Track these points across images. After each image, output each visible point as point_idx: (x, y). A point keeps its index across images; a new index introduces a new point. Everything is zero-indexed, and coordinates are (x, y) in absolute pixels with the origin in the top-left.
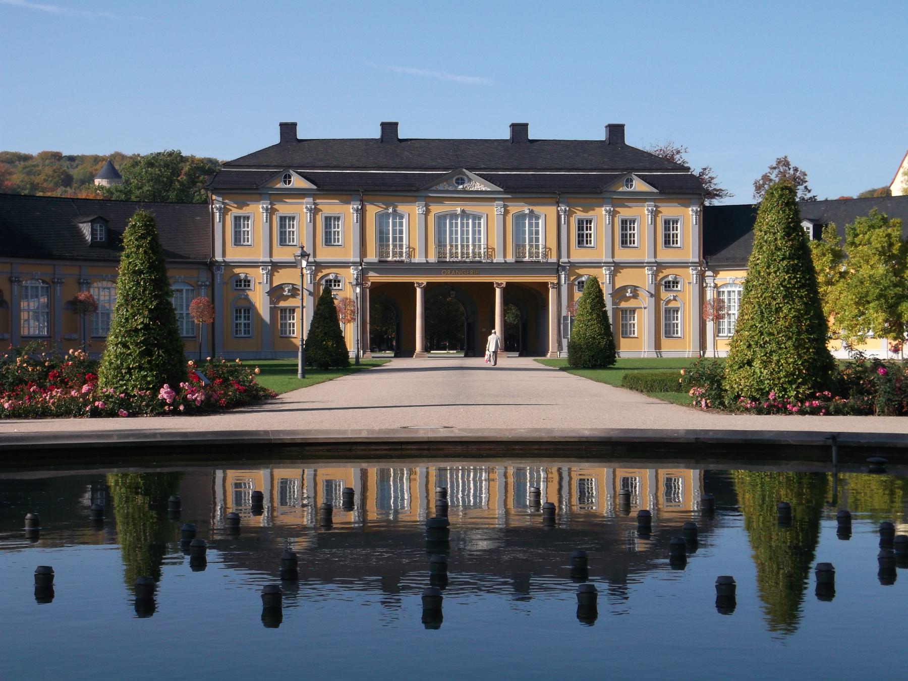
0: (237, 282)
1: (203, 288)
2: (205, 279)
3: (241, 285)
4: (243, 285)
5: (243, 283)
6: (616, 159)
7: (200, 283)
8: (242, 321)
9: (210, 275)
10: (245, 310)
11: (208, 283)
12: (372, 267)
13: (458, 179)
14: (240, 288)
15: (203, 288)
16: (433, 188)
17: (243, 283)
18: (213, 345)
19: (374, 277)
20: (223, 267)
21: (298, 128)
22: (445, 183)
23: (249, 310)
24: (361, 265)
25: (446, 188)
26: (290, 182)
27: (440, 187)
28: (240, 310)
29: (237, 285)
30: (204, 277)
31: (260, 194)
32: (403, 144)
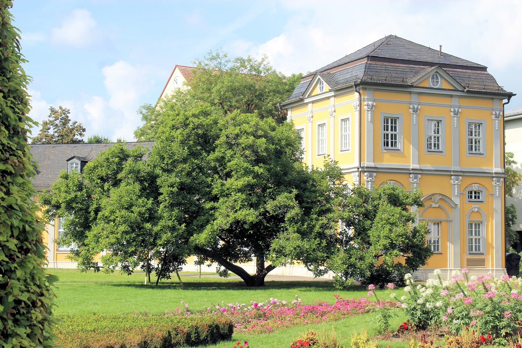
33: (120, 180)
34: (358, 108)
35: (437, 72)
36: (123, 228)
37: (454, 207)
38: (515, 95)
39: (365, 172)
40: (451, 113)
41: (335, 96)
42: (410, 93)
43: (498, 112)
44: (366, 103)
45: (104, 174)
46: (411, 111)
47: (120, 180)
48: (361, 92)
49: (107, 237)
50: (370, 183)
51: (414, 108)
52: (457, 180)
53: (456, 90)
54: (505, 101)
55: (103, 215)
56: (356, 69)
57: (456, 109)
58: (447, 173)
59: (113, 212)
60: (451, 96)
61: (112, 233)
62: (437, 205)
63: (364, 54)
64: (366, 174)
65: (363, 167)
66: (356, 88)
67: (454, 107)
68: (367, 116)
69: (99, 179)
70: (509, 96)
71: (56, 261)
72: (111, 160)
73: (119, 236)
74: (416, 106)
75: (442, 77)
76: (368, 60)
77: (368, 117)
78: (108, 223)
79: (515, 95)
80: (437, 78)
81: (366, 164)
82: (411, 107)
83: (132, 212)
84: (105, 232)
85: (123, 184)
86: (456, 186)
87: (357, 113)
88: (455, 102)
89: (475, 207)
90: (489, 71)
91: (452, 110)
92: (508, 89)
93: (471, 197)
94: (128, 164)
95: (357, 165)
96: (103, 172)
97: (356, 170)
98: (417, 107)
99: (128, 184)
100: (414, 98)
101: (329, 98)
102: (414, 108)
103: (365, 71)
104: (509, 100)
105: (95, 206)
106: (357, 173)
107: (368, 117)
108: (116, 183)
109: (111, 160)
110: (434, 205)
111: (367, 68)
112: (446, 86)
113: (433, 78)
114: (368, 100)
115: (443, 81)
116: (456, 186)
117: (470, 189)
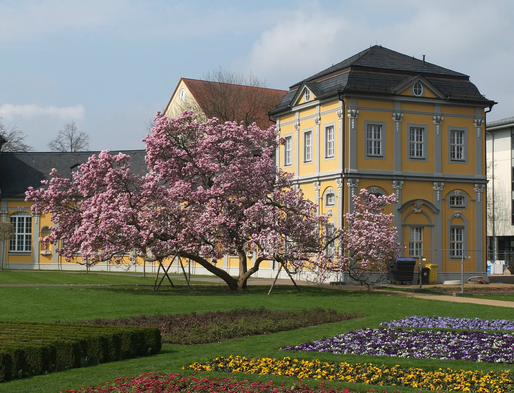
8: (25, 234)
34: (342, 116)
35: (419, 81)
37: (436, 212)
38: (497, 103)
39: (349, 178)
40: (434, 121)
41: (320, 105)
42: (393, 101)
43: (479, 120)
44: (349, 111)
46: (394, 118)
48: (345, 100)
50: (353, 189)
51: (397, 116)
52: (439, 186)
53: (438, 98)
54: (487, 109)
56: (340, 78)
57: (439, 117)
58: (430, 180)
60: (434, 104)
62: (420, 211)
63: (348, 64)
64: (349, 180)
65: (347, 174)
66: (339, 96)
67: (436, 116)
68: (351, 124)
70: (491, 104)
71: (61, 263)
74: (399, 114)
75: (424, 86)
76: (352, 69)
77: (351, 124)
79: (497, 103)
80: (420, 87)
81: (350, 170)
82: (394, 114)
86: (438, 192)
87: (341, 120)
88: (437, 110)
89: (457, 212)
90: (472, 80)
91: (435, 118)
92: (489, 97)
93: (453, 203)
95: (340, 171)
97: (340, 176)
98: (400, 115)
100: (398, 107)
101: (314, 106)
102: (397, 116)
103: (349, 80)
104: (491, 108)
106: (341, 180)
107: (351, 124)
110: (416, 210)
111: (351, 77)
112: (429, 95)
113: (415, 87)
114: (351, 109)
115: (426, 90)
116: (438, 192)
117: (452, 195)
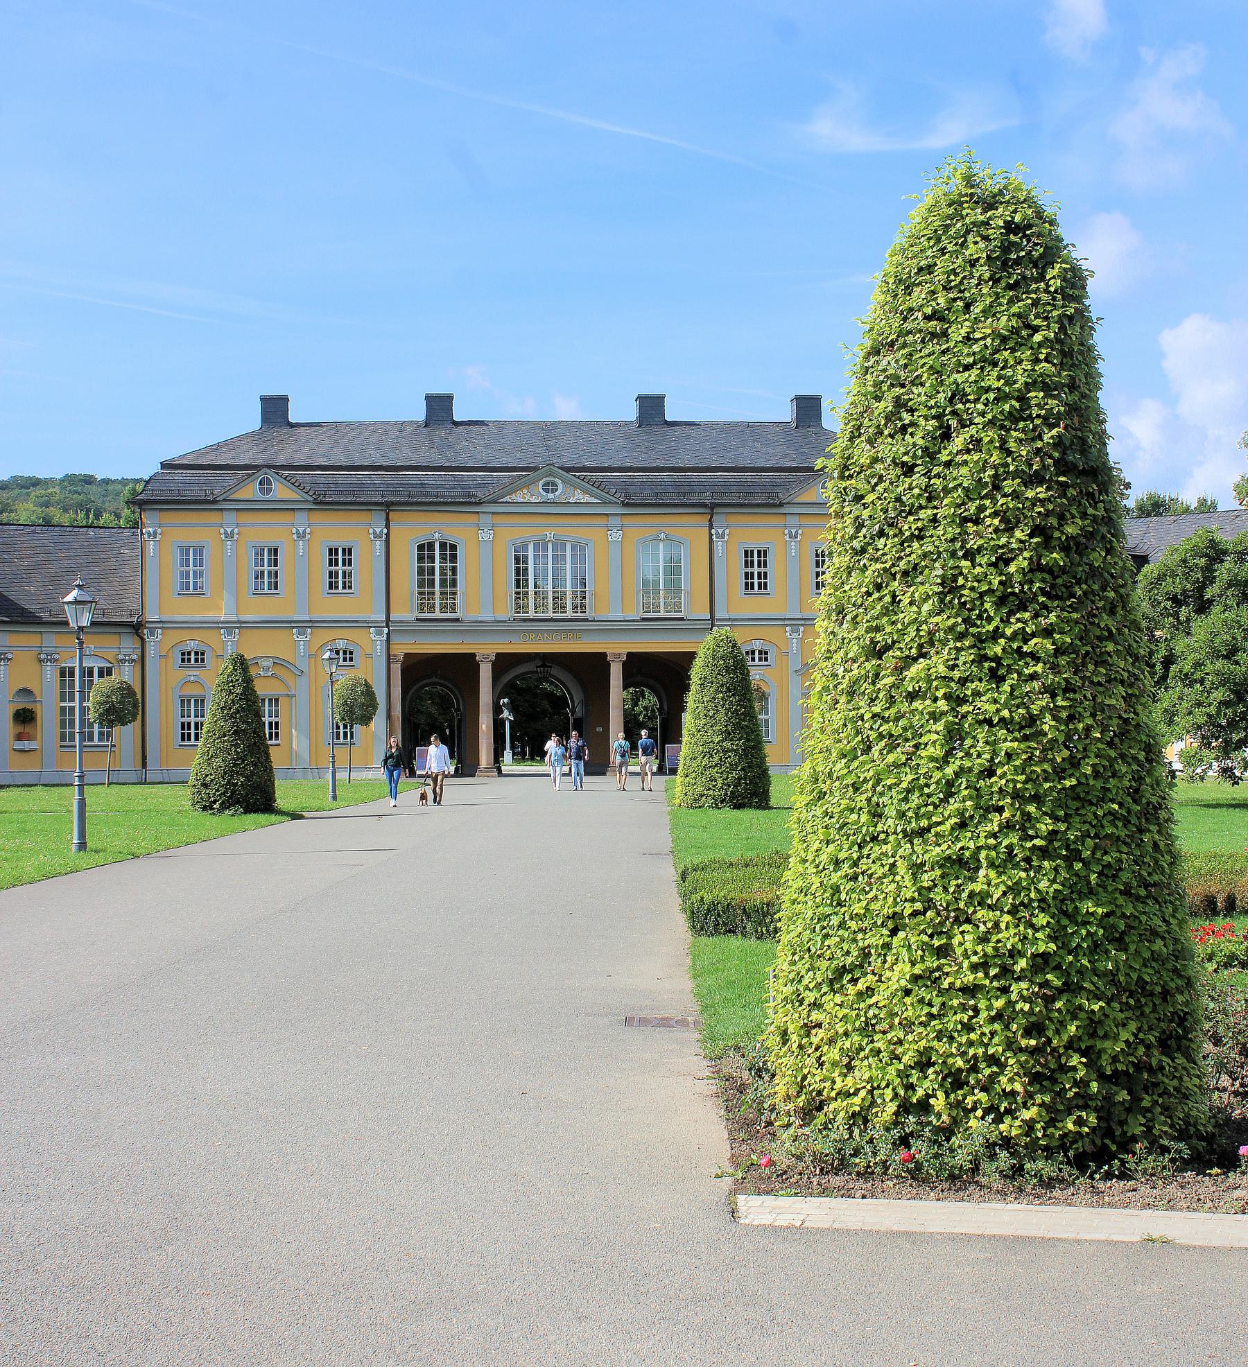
0: (183, 654)
1: (127, 664)
2: (129, 651)
3: (189, 660)
4: (193, 660)
5: (193, 657)
6: (806, 451)
7: (121, 657)
9: (138, 644)
10: (196, 701)
11: (134, 657)
12: (406, 629)
13: (546, 484)
14: (188, 665)
15: (127, 664)
16: (504, 500)
17: (193, 657)
18: (144, 758)
19: (405, 646)
20: (160, 631)
21: (291, 405)
22: (525, 491)
23: (203, 701)
24: (388, 626)
25: (528, 498)
26: (269, 490)
27: (517, 497)
28: (189, 701)
29: (183, 660)
30: (129, 645)
31: (221, 510)
32: (461, 429)
33: (1211, 602)
36: (1219, 695)
45: (1179, 590)
47: (1211, 602)
49: (1190, 713)
55: (1180, 671)
59: (1198, 664)
61: (1199, 704)
69: (1168, 599)
72: (1191, 563)
73: (1212, 710)
78: (1191, 685)
83: (1237, 663)
84: (1185, 704)
85: (1216, 609)
94: (1224, 571)
96: (1176, 586)
99: (1226, 608)
105: (1163, 653)
108: (1203, 607)
109: (1191, 563)
